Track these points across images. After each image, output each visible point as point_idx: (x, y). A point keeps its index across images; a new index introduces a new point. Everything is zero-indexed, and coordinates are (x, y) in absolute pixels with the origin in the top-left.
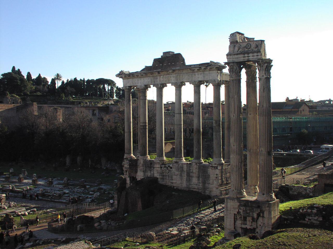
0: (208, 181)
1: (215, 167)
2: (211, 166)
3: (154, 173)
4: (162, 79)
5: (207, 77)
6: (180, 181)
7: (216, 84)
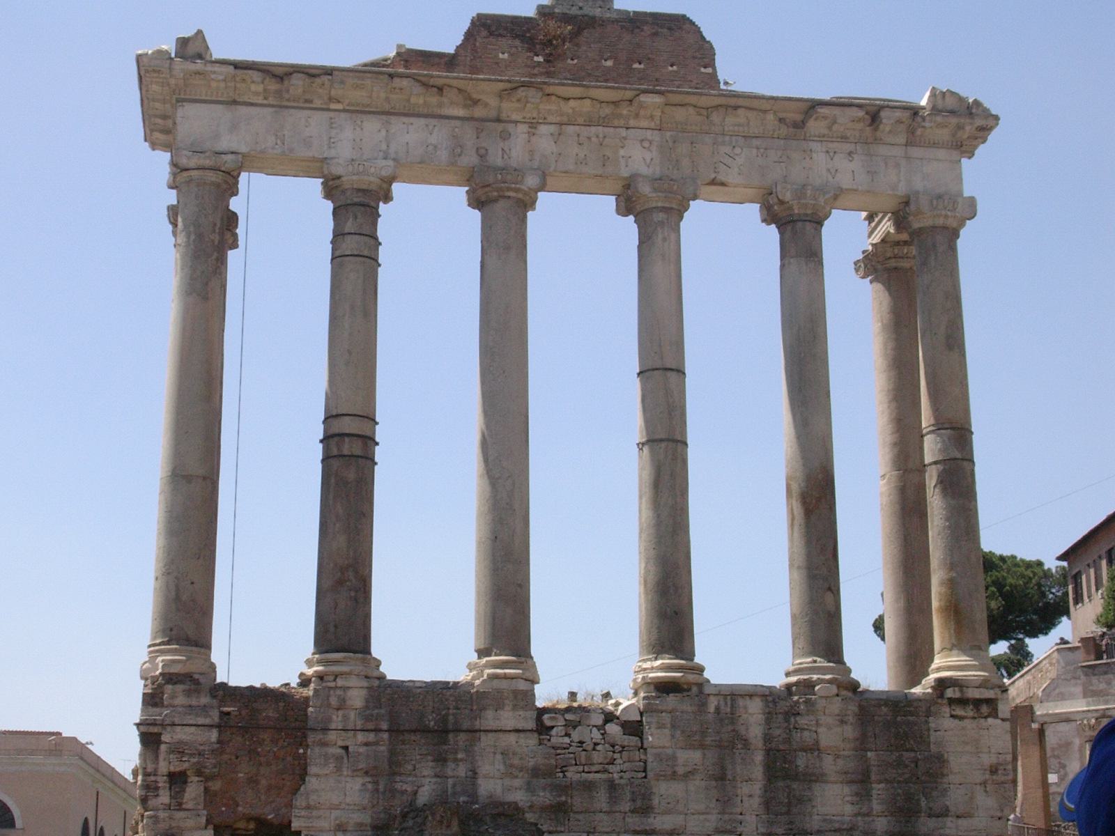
0: (935, 793)
1: (977, 703)
2: (958, 695)
3: (474, 773)
4: (545, 142)
6: (713, 817)
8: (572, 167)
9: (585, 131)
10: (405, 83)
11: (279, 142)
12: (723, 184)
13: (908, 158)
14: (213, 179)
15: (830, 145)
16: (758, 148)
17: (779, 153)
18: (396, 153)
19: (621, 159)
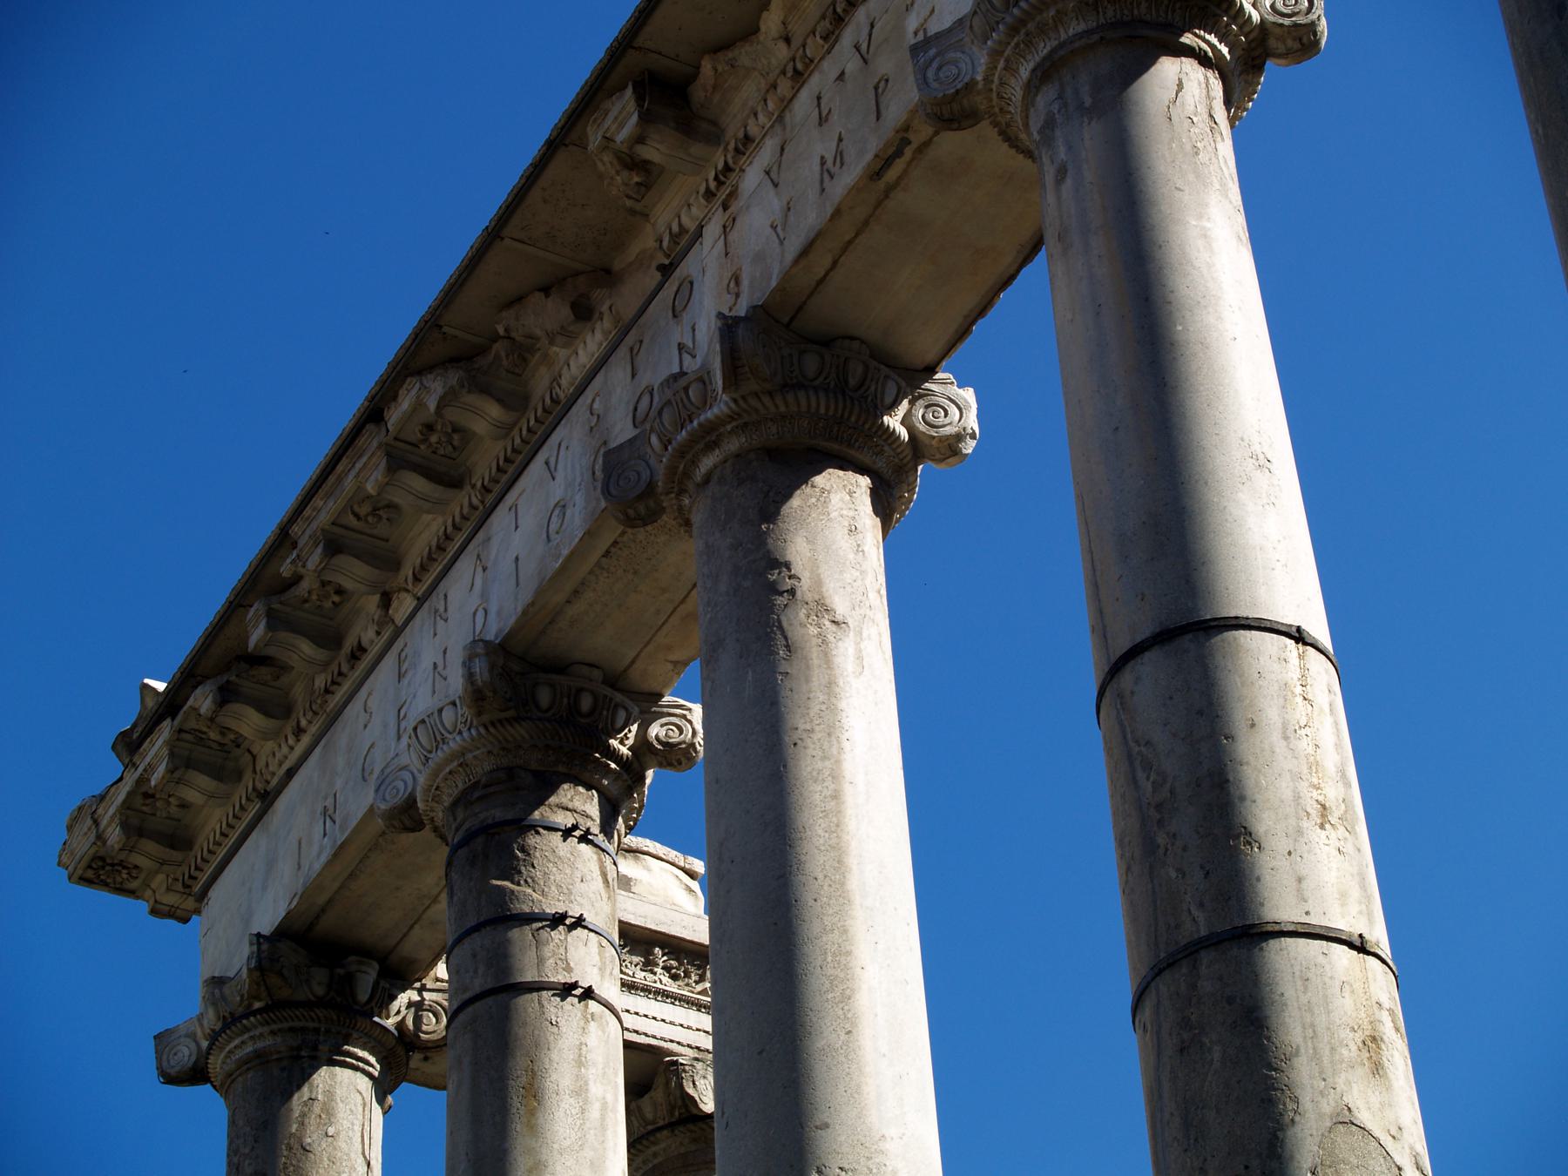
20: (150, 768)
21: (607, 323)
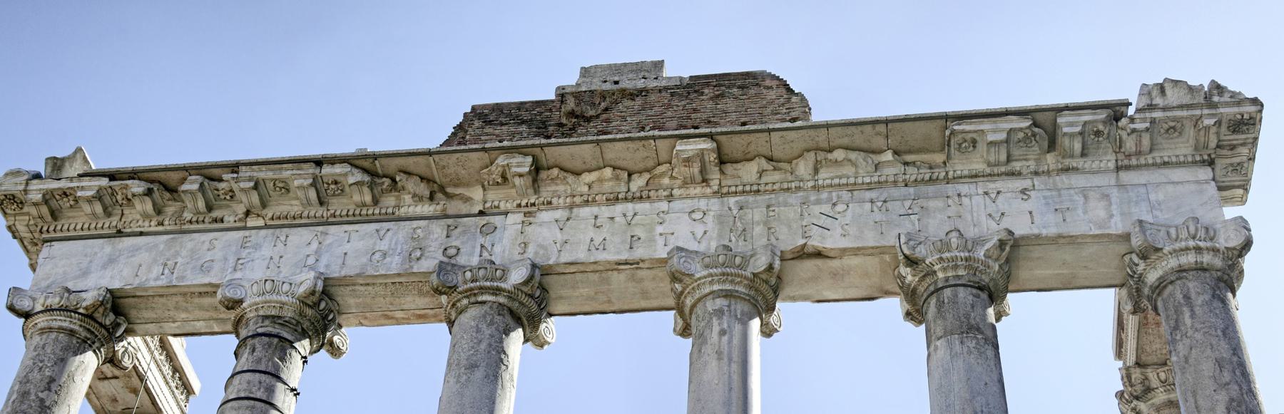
5: (1102, 214)
7: (1218, 262)
8: (581, 255)
9: (605, 212)
10: (338, 169)
11: (166, 271)
12: (818, 254)
13: (1120, 186)
14: (65, 325)
15: (992, 185)
16: (872, 202)
17: (907, 204)
18: (327, 266)
19: (658, 237)
20: (83, 188)
21: (439, 208)
